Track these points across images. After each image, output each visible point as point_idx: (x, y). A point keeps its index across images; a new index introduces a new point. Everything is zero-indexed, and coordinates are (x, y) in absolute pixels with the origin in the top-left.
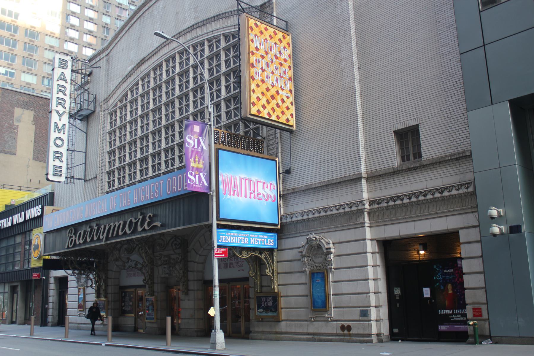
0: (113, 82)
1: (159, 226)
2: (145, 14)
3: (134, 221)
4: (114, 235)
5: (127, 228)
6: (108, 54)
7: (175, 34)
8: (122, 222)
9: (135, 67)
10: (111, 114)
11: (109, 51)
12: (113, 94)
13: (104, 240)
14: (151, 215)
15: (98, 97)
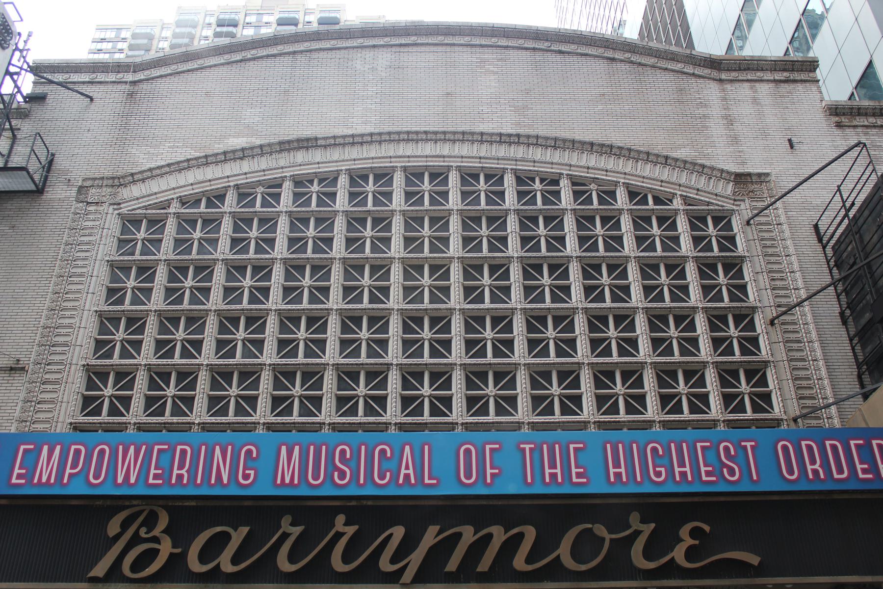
0: (152, 150)
1: (756, 564)
2: (315, 55)
3: (601, 530)
4: (485, 565)
5: (564, 551)
6: (134, 83)
7: (432, 129)
8: (530, 533)
9: (270, 145)
10: (131, 222)
11: (140, 76)
12: (152, 177)
13: (408, 576)
14: (707, 528)
15: (61, 162)
